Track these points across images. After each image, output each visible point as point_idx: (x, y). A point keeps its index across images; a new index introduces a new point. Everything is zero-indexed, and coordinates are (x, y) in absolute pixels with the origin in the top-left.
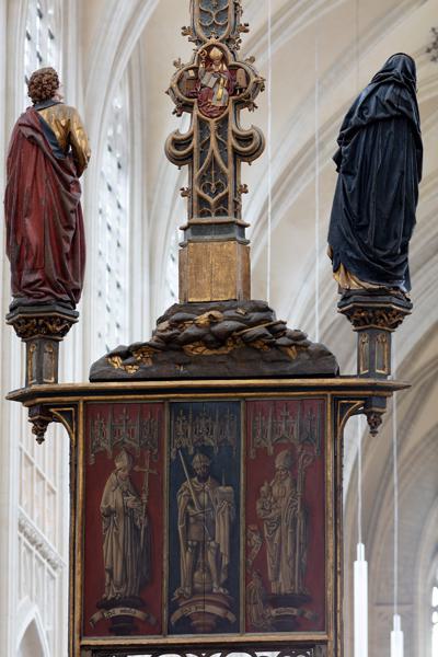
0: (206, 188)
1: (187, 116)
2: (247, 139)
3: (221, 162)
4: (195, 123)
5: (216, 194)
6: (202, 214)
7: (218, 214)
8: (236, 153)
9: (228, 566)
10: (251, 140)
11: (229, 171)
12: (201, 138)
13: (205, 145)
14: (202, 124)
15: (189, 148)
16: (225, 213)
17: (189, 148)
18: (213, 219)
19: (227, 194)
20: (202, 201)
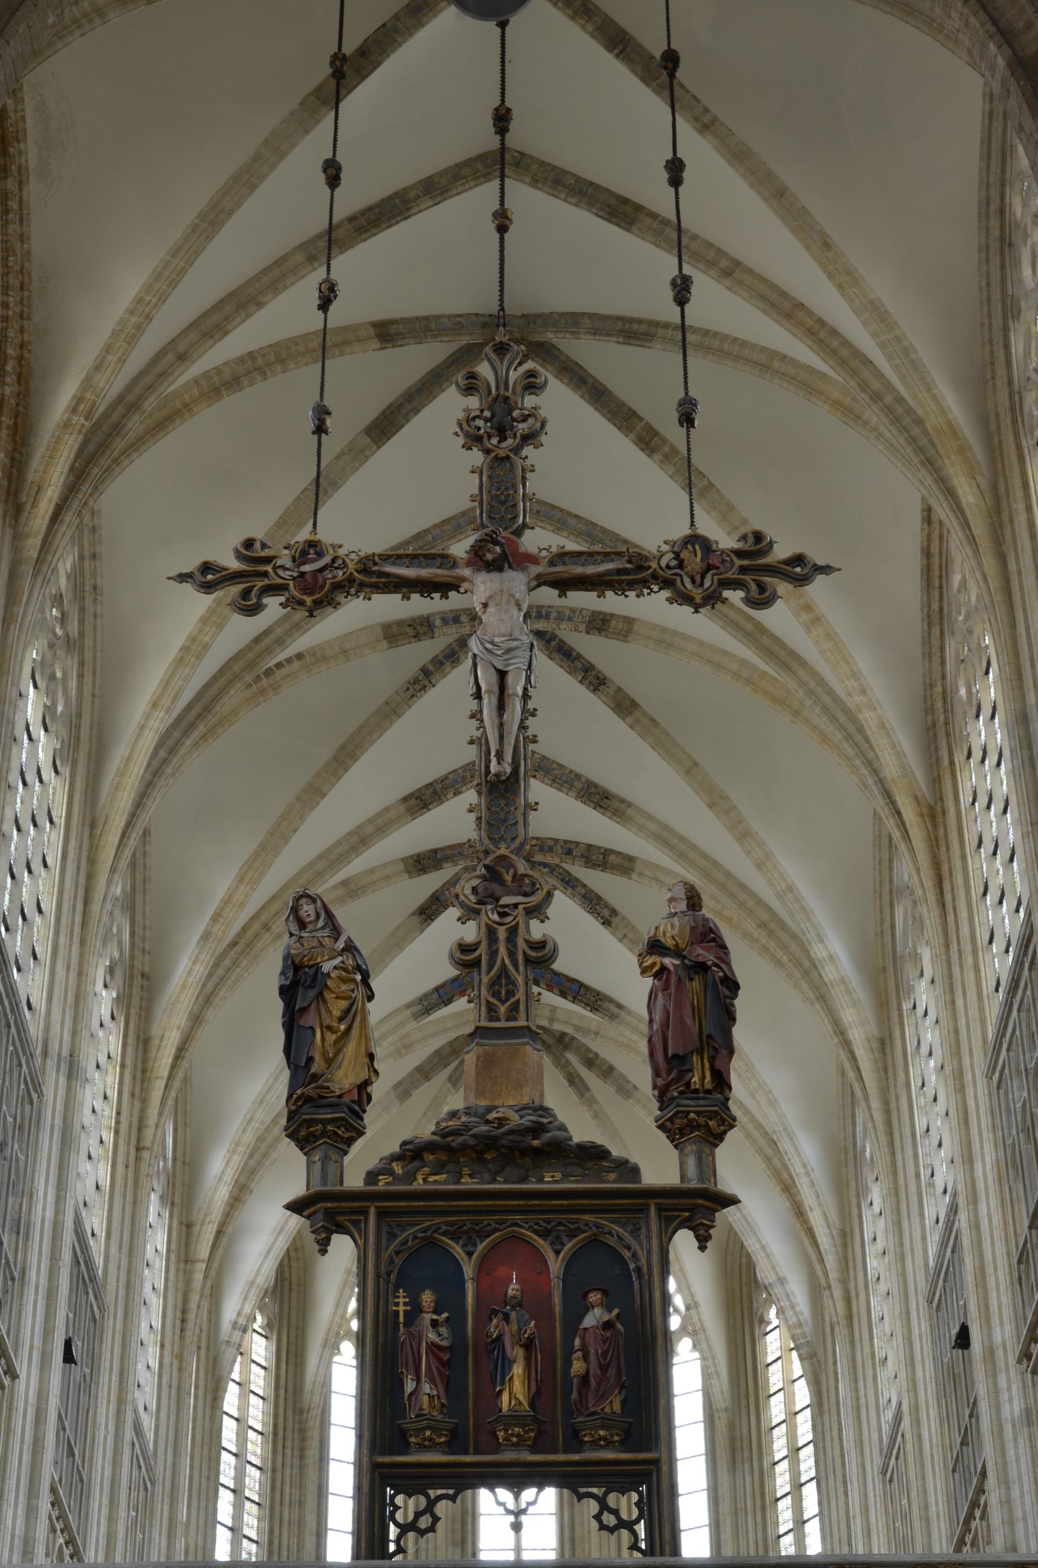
0: (496, 994)
1: (472, 925)
2: (541, 945)
3: (510, 967)
4: (483, 929)
5: (507, 1000)
6: (491, 1020)
7: (508, 1020)
8: (527, 960)
9: (531, 1146)
10: (544, 947)
11: (520, 980)
12: (490, 946)
13: (493, 954)
14: (491, 933)
15: (476, 954)
16: (516, 1019)
17: (476, 954)
18: (502, 1024)
19: (518, 1001)
20: (491, 1009)
